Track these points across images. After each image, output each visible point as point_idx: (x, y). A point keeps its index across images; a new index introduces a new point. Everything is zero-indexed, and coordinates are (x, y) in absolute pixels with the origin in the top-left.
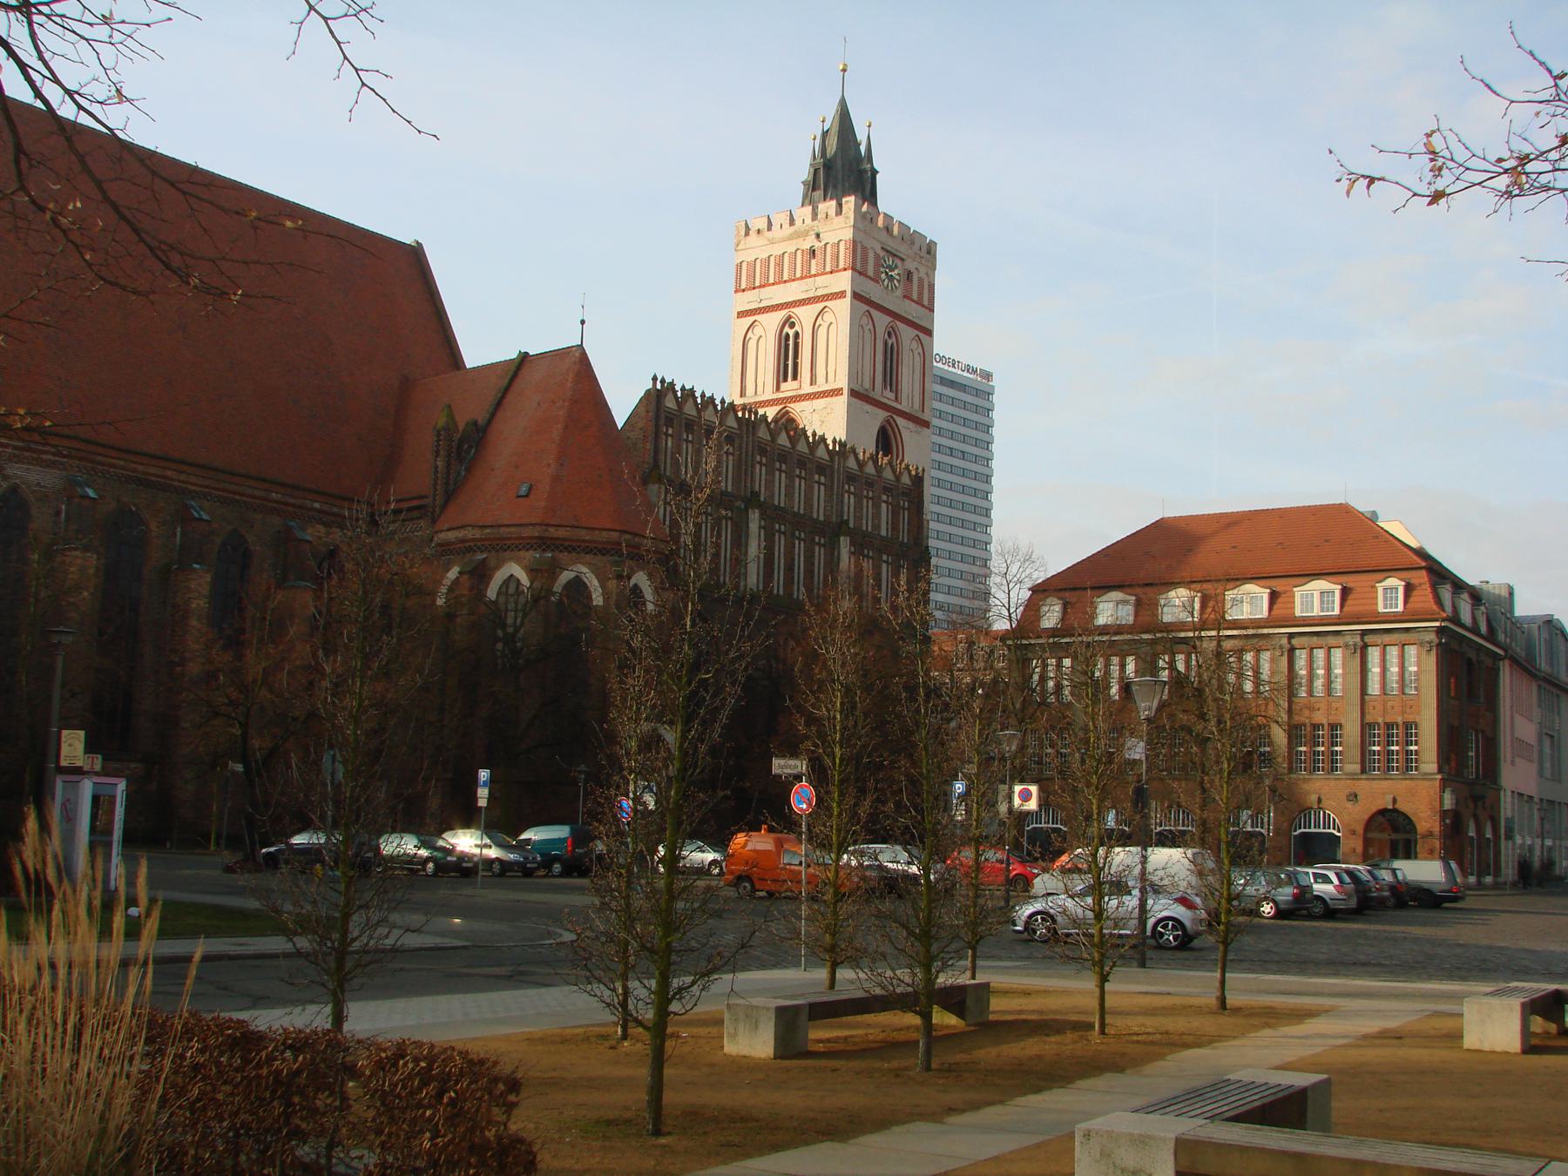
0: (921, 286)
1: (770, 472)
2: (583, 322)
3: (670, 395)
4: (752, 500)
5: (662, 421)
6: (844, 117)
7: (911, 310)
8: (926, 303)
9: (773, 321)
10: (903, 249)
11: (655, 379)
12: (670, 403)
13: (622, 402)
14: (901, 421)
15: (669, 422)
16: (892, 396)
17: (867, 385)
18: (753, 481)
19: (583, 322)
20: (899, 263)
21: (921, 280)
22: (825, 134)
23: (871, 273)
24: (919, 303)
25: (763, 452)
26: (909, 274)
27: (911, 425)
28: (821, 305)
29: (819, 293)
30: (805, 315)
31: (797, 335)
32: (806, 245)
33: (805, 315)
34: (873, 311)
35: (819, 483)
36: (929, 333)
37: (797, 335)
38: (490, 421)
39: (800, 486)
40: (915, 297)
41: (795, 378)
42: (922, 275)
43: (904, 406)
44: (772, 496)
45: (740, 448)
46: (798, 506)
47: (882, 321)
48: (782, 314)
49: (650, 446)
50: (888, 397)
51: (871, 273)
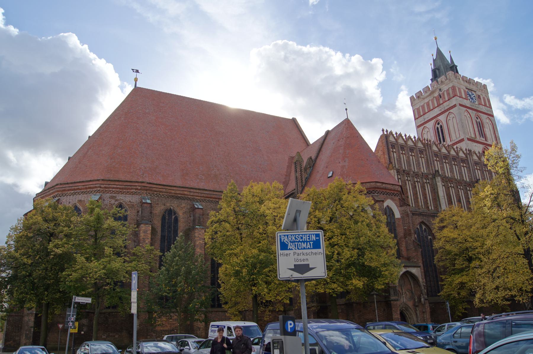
1: (442, 163)
2: (346, 109)
3: (391, 136)
4: (436, 174)
5: (390, 146)
6: (439, 53)
7: (483, 109)
8: (488, 105)
9: (430, 125)
10: (474, 88)
11: (383, 130)
12: (391, 139)
13: (372, 140)
15: (393, 147)
17: (473, 136)
18: (435, 167)
19: (346, 109)
20: (474, 93)
21: (484, 98)
22: (434, 60)
23: (464, 97)
24: (485, 105)
25: (436, 156)
26: (479, 96)
29: (446, 108)
30: (442, 118)
31: (441, 127)
32: (436, 94)
33: (442, 118)
34: (468, 110)
36: (493, 116)
37: (441, 127)
38: (317, 157)
39: (455, 169)
40: (483, 104)
42: (484, 96)
44: (445, 173)
45: (426, 154)
46: (457, 176)
47: (473, 113)
48: (433, 121)
49: (386, 156)
50: (482, 140)
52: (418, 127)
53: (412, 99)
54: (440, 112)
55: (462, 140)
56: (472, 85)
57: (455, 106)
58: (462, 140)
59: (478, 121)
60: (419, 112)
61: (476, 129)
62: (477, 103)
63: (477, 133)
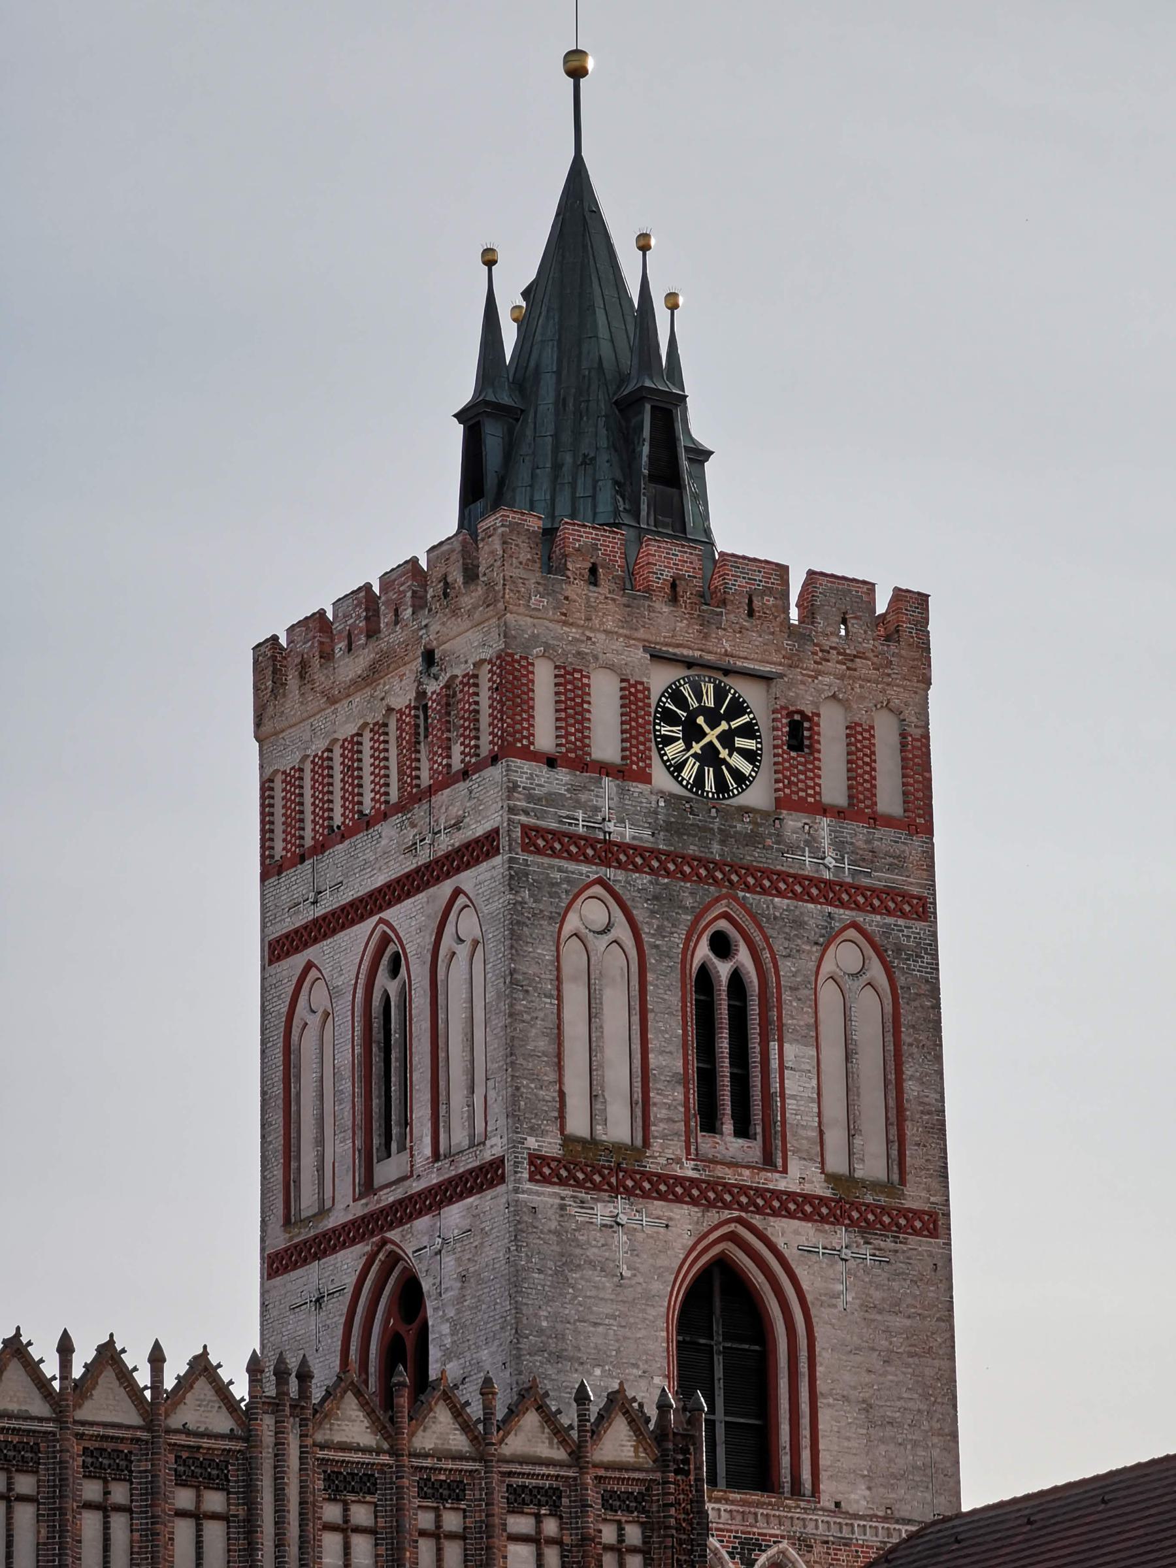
6: (578, 218)
7: (820, 849)
8: (889, 800)
14: (790, 1234)
16: (746, 1150)
21: (859, 740)
23: (606, 745)
26: (799, 734)
27: (840, 1237)
28: (445, 889)
29: (446, 843)
30: (409, 919)
35: (198, 1516)
40: (834, 790)
41: (402, 1148)
43: (799, 1176)
51: (606, 745)
52: (277, 949)
53: (273, 665)
54: (409, 865)
55: (488, 1175)
56: (735, 615)
57: (482, 848)
58: (488, 1175)
59: (723, 970)
60: (295, 820)
61: (671, 1057)
62: (757, 796)
63: (672, 1100)
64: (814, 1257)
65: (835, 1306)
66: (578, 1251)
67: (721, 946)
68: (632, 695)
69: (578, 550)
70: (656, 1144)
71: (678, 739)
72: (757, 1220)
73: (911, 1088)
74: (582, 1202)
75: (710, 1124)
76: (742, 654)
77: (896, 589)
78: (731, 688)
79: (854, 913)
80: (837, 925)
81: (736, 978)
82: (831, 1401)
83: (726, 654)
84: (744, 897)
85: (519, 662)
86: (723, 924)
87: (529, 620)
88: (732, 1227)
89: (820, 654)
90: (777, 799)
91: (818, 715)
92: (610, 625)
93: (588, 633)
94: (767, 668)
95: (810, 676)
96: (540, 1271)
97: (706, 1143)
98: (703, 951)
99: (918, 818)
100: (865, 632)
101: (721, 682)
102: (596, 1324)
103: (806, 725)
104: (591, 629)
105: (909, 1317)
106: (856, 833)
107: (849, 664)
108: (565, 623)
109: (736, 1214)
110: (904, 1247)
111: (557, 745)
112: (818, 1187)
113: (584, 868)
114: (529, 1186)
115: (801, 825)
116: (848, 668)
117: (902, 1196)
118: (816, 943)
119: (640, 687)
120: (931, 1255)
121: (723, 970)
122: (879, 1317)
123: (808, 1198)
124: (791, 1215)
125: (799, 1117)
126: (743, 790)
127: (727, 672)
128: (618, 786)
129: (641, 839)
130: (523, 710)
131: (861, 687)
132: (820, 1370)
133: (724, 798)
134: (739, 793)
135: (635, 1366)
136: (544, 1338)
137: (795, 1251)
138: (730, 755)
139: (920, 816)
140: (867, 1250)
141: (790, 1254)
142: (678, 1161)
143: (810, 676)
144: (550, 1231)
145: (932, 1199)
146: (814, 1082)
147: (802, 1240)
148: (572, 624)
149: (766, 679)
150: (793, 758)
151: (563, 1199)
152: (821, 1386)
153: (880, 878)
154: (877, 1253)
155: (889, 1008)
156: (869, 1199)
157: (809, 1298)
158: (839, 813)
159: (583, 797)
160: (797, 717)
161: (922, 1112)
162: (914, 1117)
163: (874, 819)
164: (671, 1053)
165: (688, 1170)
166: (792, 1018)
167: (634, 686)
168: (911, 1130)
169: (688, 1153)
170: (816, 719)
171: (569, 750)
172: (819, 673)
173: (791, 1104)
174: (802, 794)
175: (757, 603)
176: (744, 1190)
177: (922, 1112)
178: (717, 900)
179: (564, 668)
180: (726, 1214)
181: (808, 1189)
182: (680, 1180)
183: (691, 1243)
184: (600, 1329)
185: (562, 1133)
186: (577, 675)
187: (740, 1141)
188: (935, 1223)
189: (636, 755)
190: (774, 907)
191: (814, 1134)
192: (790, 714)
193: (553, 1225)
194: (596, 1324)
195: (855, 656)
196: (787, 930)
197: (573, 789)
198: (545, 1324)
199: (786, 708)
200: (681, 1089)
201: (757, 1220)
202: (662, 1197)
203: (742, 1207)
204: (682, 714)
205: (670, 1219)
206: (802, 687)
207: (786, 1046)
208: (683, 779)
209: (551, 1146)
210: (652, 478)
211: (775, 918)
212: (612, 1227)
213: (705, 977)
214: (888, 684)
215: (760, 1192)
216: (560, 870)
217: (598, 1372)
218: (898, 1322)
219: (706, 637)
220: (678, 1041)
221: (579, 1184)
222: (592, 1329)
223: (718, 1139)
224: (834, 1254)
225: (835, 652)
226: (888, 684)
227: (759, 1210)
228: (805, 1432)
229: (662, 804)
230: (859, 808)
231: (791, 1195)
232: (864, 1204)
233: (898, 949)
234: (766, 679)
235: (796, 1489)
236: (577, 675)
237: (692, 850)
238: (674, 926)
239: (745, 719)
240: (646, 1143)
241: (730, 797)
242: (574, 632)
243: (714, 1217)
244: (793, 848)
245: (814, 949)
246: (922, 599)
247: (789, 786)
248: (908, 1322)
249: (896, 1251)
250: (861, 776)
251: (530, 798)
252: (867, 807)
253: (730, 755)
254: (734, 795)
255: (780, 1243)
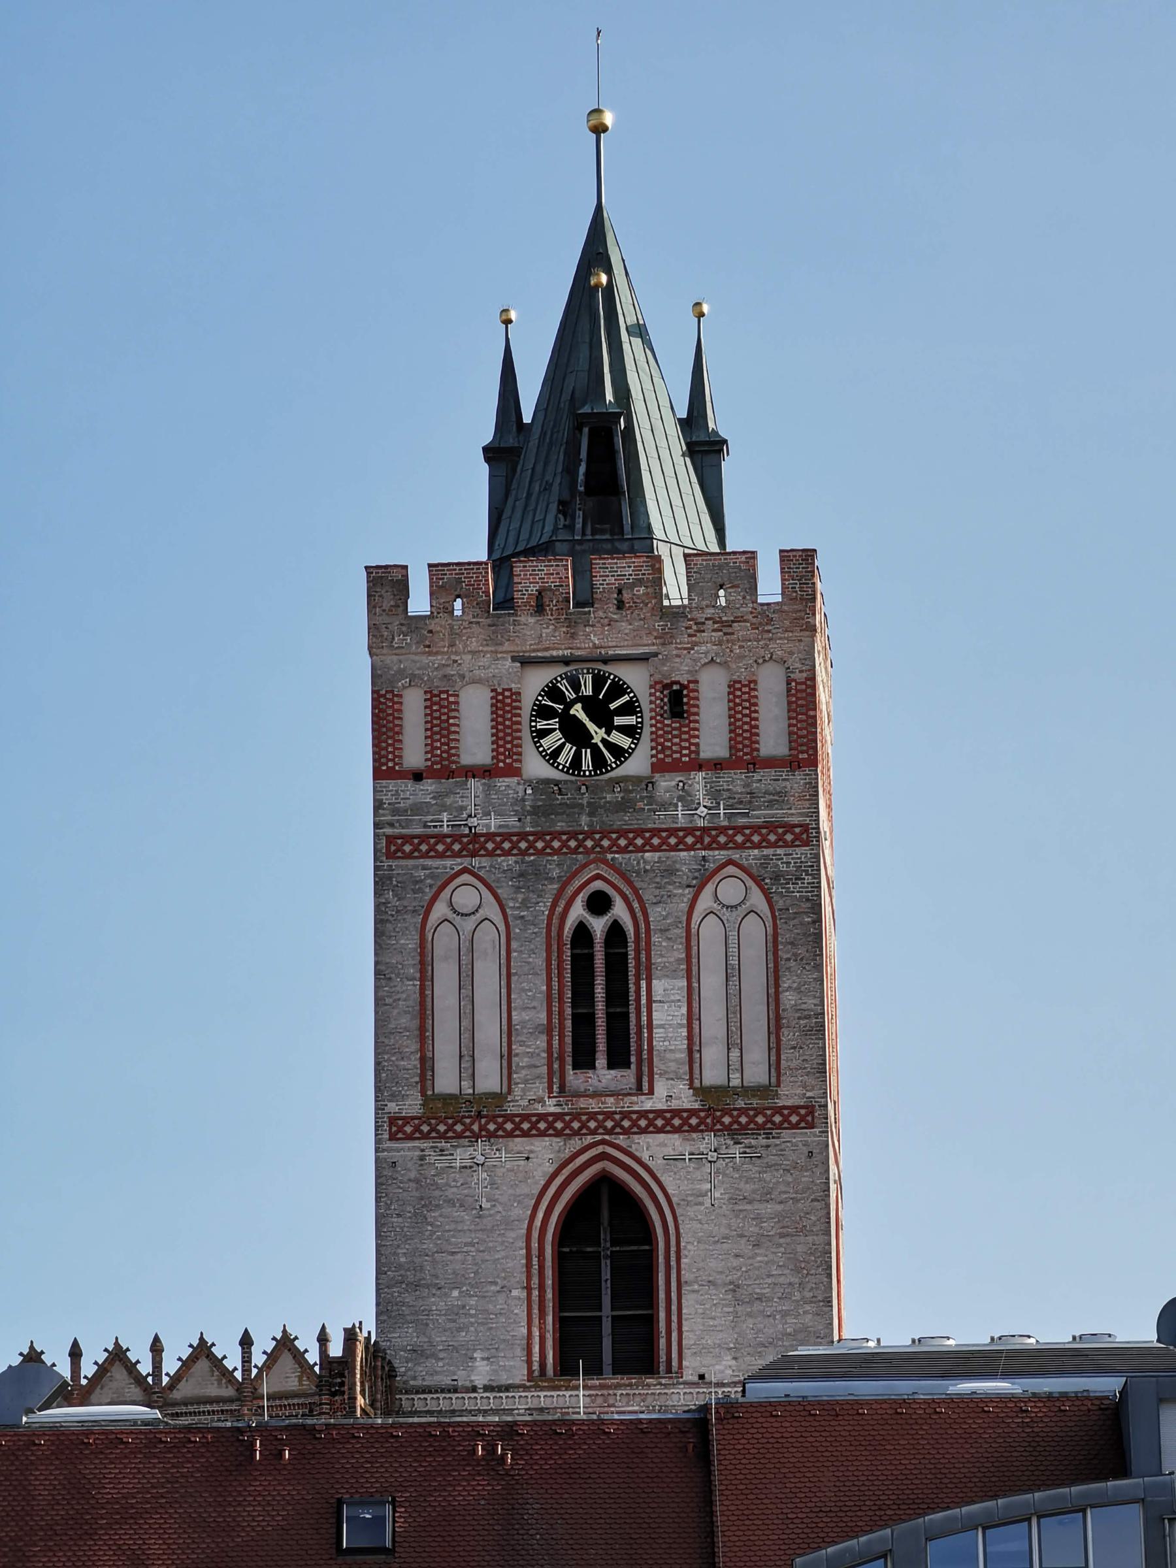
0: (742, 698)
14: (653, 1148)
16: (624, 1078)
26: (677, 702)
27: (707, 1142)
59: (598, 926)
62: (637, 764)
63: (533, 1049)
64: (680, 1164)
65: (701, 1204)
66: (437, 1193)
67: (599, 903)
68: (503, 704)
69: (442, 587)
70: (517, 1091)
71: (555, 730)
72: (621, 1140)
73: (789, 999)
74: (442, 1150)
75: (584, 1059)
76: (610, 644)
77: (781, 551)
78: (610, 674)
79: (730, 852)
80: (712, 866)
81: (616, 932)
82: (696, 1287)
83: (595, 647)
84: (613, 859)
85: (384, 696)
86: (598, 885)
87: (395, 658)
88: (600, 1149)
89: (695, 627)
90: (653, 764)
91: (697, 682)
92: (474, 645)
93: (453, 657)
94: (646, 650)
95: (685, 649)
96: (399, 1215)
97: (575, 1079)
98: (578, 911)
99: (804, 753)
100: (744, 598)
101: (599, 671)
102: (453, 1253)
103: (685, 692)
104: (456, 653)
105: (781, 1203)
106: (735, 781)
107: (726, 630)
108: (430, 654)
109: (599, 1137)
110: (777, 1141)
111: (426, 760)
112: (686, 1099)
113: (449, 862)
114: (389, 1144)
115: (674, 783)
116: (725, 634)
117: (777, 1095)
118: (689, 886)
119: (507, 693)
120: (806, 1144)
121: (598, 926)
122: (748, 1207)
123: (676, 1113)
124: (660, 1131)
125: (666, 1043)
126: (622, 763)
127: (605, 661)
128: (484, 784)
129: (507, 826)
130: (389, 737)
131: (740, 647)
132: (684, 1261)
133: (602, 773)
134: (618, 766)
135: (495, 1283)
136: (402, 1272)
137: (661, 1161)
138: (608, 733)
139: (802, 752)
140: (736, 1150)
141: (656, 1165)
142: (541, 1100)
143: (685, 649)
144: (410, 1180)
145: (809, 1094)
146: (684, 1010)
147: (669, 1151)
148: (437, 653)
149: (643, 659)
150: (668, 725)
151: (423, 1150)
152: (686, 1275)
153: (760, 815)
154: (748, 1150)
155: (770, 930)
156: (740, 1103)
157: (675, 1200)
158: (717, 765)
159: (448, 801)
160: (675, 687)
161: (799, 1018)
162: (798, 1026)
163: (754, 764)
164: (534, 1008)
165: (551, 1107)
166: (661, 956)
167: (502, 694)
168: (787, 1036)
169: (550, 1091)
170: (692, 686)
171: (433, 763)
172: (696, 644)
173: (658, 1033)
174: (678, 755)
175: (626, 596)
176: (609, 1115)
177: (799, 1018)
178: (585, 866)
179: (431, 692)
180: (589, 1139)
181: (675, 1104)
182: (542, 1117)
183: (551, 1170)
184: (459, 1257)
185: (423, 1092)
186: (444, 696)
187: (612, 1072)
188: (812, 1116)
189: (503, 754)
190: (645, 862)
191: (683, 1056)
192: (666, 687)
193: (413, 1175)
194: (453, 1253)
195: (733, 622)
196: (658, 880)
197: (437, 796)
198: (403, 1260)
199: (661, 682)
200: (544, 1038)
201: (621, 1140)
202: (526, 1134)
203: (610, 1132)
204: (559, 707)
205: (531, 1152)
206: (678, 660)
207: (654, 982)
208: (559, 764)
209: (412, 1105)
210: (589, 491)
211: (646, 871)
212: (471, 1167)
213: (582, 933)
214: (770, 639)
215: (626, 1115)
216: (424, 868)
217: (456, 1293)
218: (770, 1208)
219: (573, 636)
220: (542, 997)
221: (443, 1136)
222: (450, 1257)
223: (590, 1073)
224: (698, 1158)
225: (711, 622)
226: (770, 639)
227: (626, 1132)
228: (674, 1318)
229: (529, 791)
230: (743, 755)
231: (659, 1113)
232: (735, 1109)
233: (776, 877)
234: (643, 659)
235: (669, 1370)
236: (444, 696)
237: (560, 826)
238: (539, 896)
239: (626, 698)
240: (510, 1091)
241: (607, 771)
242: (439, 660)
243: (576, 1144)
244: (664, 806)
245: (687, 891)
246: (809, 555)
247: (662, 751)
248: (779, 1208)
249: (768, 1146)
250: (740, 727)
251: (395, 811)
252: (746, 754)
253: (608, 733)
254: (613, 769)
255: (645, 1157)
